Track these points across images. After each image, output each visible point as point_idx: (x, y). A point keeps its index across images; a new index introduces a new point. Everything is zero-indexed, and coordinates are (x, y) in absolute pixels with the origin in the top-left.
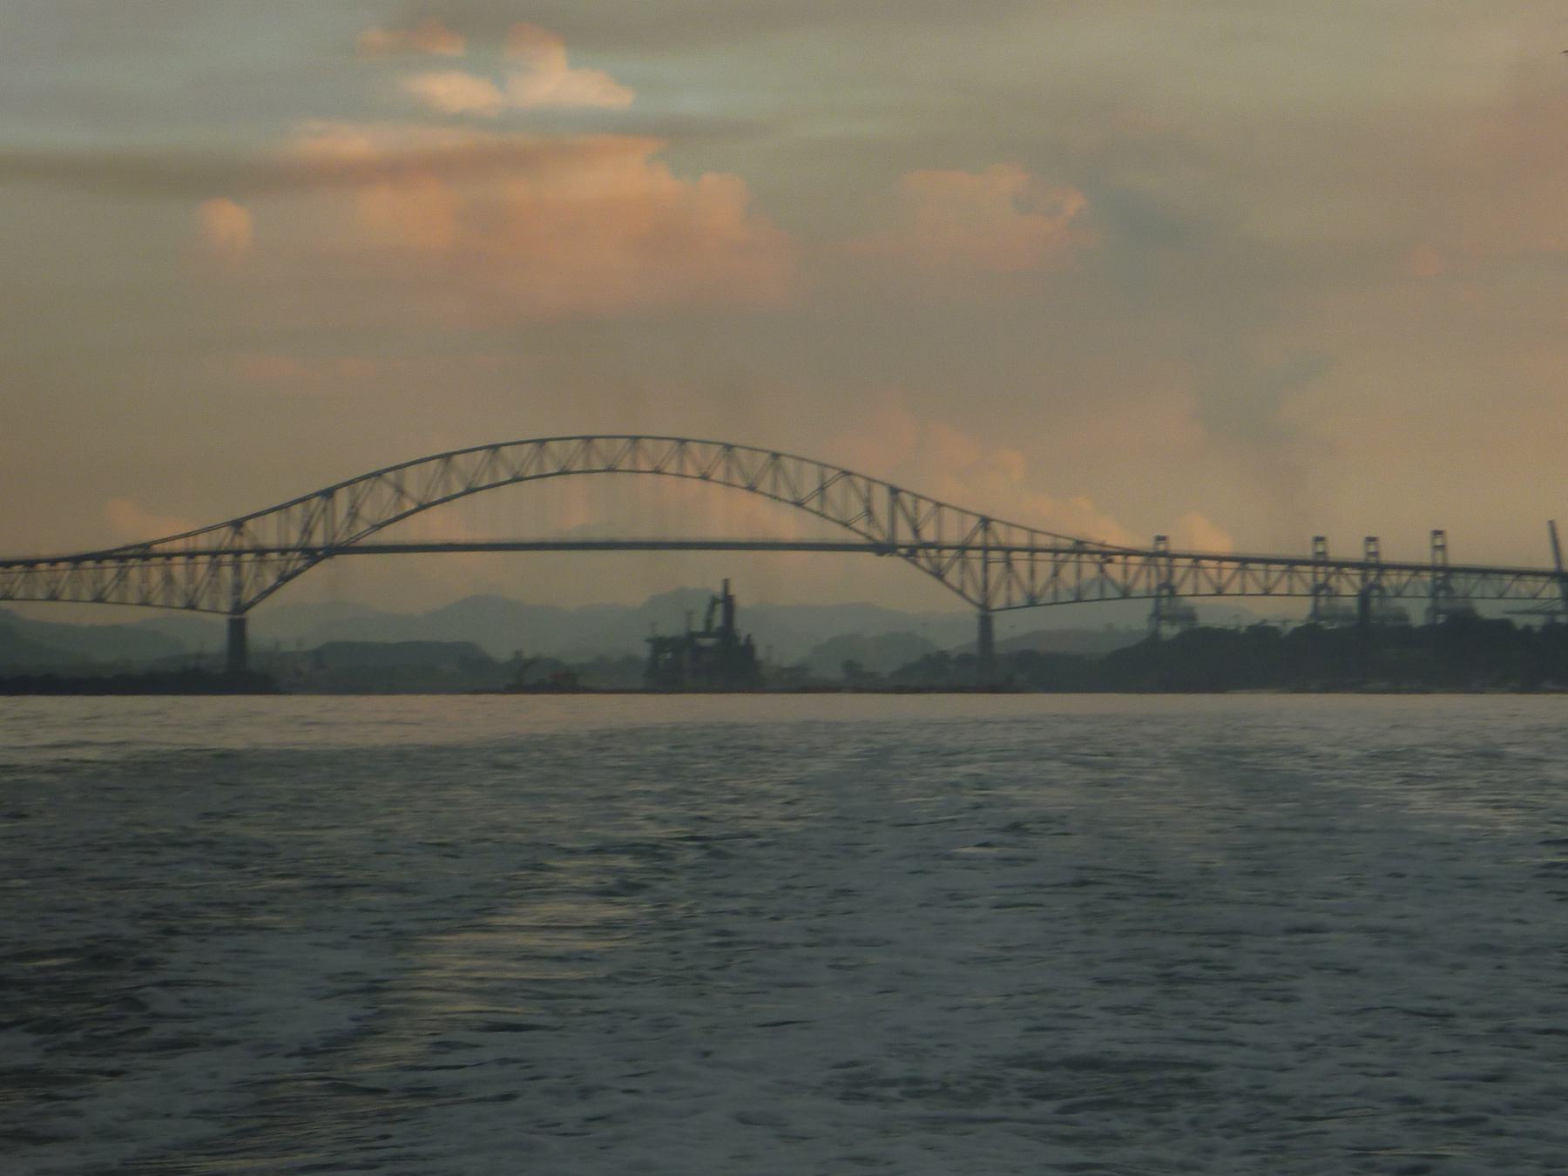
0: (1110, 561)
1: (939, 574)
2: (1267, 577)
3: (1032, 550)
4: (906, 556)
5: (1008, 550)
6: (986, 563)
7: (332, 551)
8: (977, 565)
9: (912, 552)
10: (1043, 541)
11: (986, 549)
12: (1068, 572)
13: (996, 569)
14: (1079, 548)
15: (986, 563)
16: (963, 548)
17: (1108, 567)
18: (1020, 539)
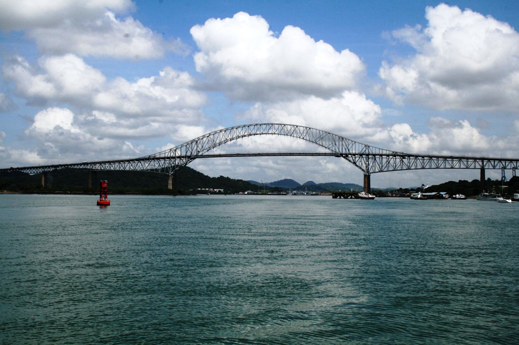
0: (405, 158)
1: (355, 163)
2: (467, 164)
3: (381, 155)
4: (344, 157)
5: (374, 155)
6: (368, 161)
7: (197, 157)
8: (365, 159)
9: (346, 156)
10: (384, 152)
11: (368, 155)
12: (392, 162)
13: (370, 160)
14: (395, 155)
15: (368, 161)
16: (361, 155)
17: (404, 160)
18: (378, 152)
